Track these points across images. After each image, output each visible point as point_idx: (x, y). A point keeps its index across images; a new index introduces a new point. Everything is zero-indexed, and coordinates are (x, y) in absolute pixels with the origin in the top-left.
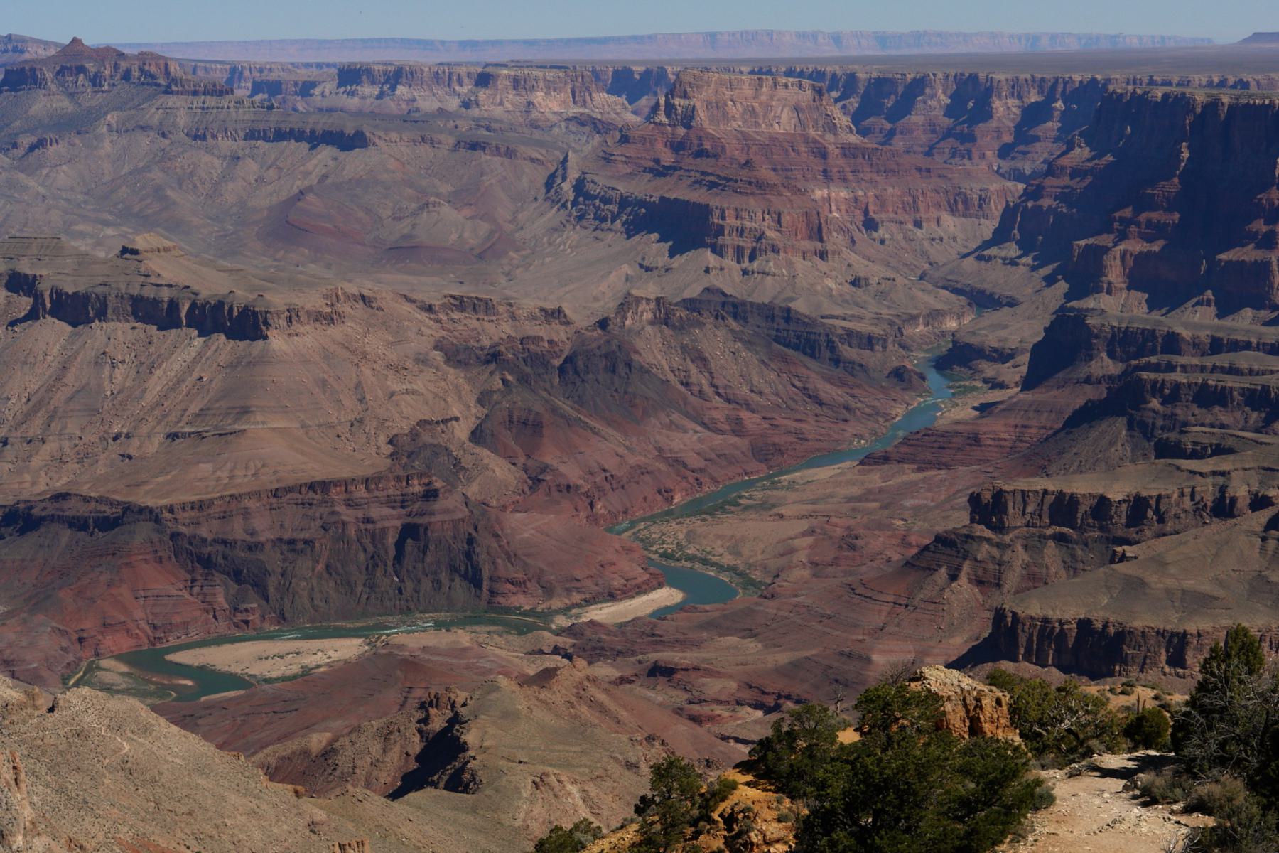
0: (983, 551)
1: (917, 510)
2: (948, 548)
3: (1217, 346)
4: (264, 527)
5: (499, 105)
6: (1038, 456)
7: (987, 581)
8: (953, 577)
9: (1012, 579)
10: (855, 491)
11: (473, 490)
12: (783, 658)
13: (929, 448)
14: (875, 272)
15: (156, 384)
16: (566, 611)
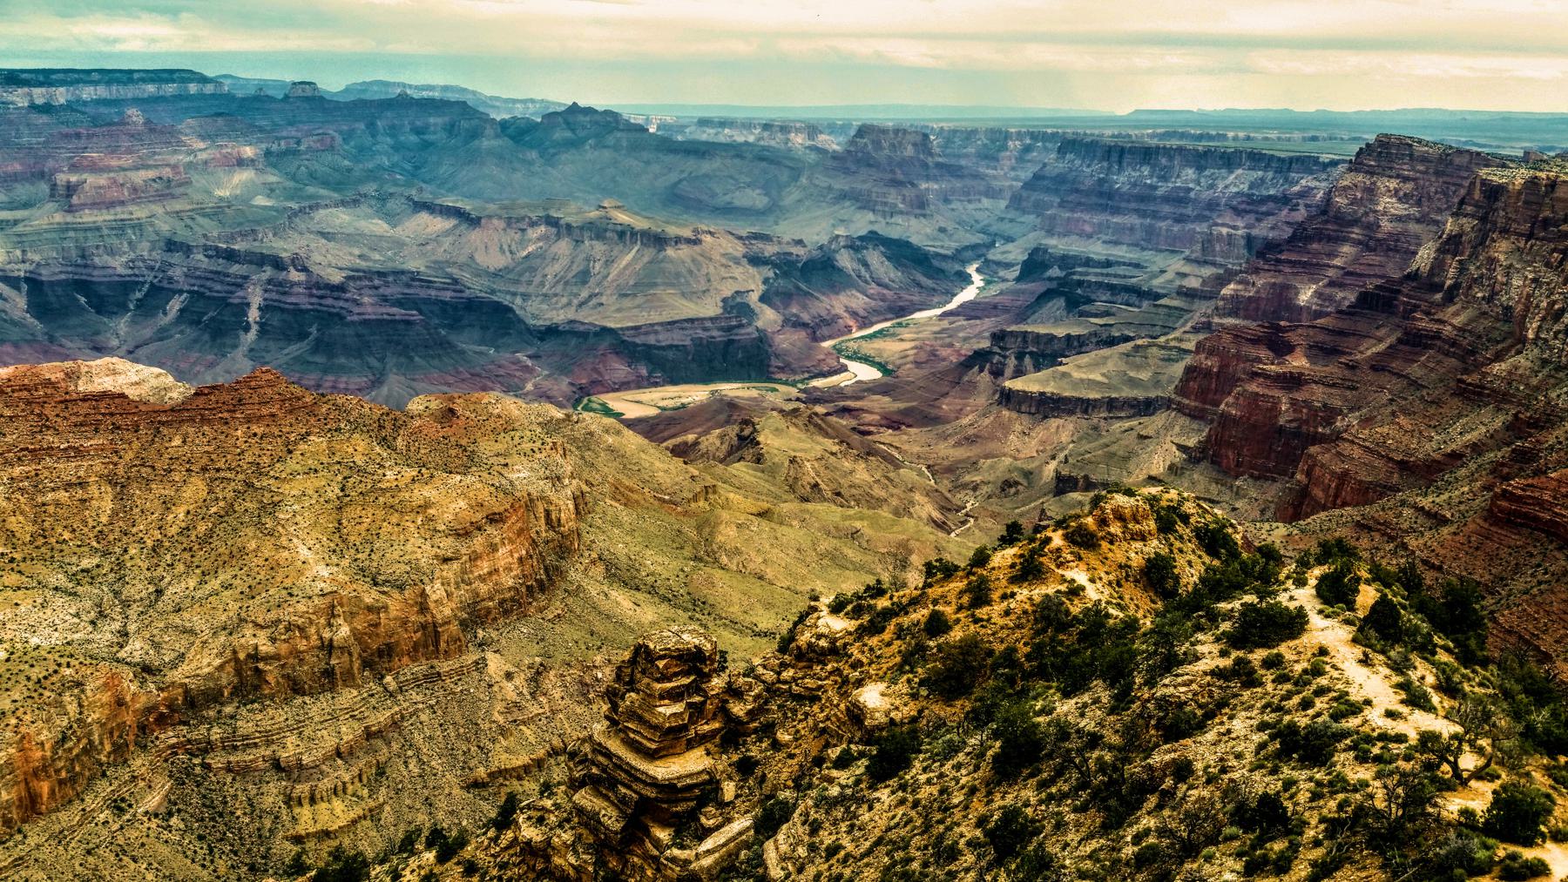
0: (996, 359)
1: (965, 339)
2: (979, 358)
3: (1108, 264)
4: (665, 338)
5: (775, 141)
6: (1022, 315)
7: (997, 373)
8: (981, 370)
9: (1009, 371)
10: (936, 329)
11: (759, 324)
12: (902, 405)
13: (970, 311)
14: (950, 226)
15: (614, 273)
16: (802, 381)
